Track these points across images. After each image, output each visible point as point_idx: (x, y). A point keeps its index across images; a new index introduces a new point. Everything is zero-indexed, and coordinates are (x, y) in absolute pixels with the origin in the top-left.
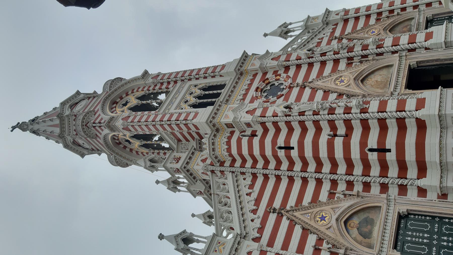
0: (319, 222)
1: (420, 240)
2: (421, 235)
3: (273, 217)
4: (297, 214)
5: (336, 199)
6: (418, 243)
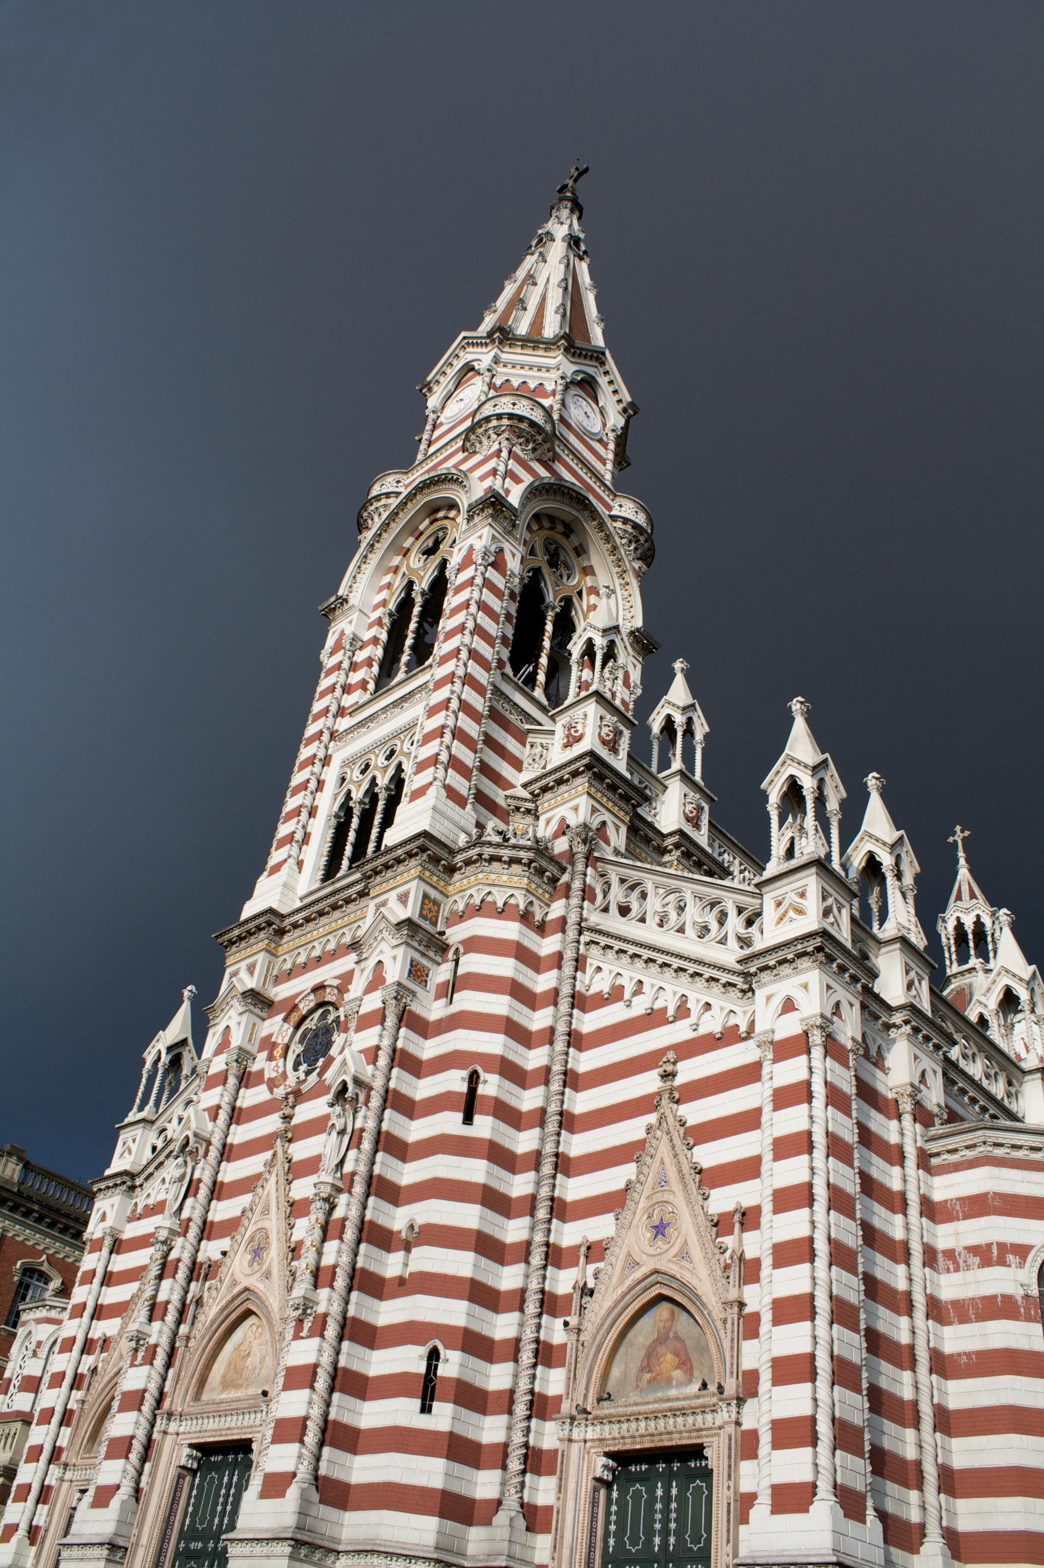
1: (658, 1526)
2: (673, 1525)
3: (648, 1082)
4: (663, 1150)
5: (719, 1240)
6: (650, 1521)
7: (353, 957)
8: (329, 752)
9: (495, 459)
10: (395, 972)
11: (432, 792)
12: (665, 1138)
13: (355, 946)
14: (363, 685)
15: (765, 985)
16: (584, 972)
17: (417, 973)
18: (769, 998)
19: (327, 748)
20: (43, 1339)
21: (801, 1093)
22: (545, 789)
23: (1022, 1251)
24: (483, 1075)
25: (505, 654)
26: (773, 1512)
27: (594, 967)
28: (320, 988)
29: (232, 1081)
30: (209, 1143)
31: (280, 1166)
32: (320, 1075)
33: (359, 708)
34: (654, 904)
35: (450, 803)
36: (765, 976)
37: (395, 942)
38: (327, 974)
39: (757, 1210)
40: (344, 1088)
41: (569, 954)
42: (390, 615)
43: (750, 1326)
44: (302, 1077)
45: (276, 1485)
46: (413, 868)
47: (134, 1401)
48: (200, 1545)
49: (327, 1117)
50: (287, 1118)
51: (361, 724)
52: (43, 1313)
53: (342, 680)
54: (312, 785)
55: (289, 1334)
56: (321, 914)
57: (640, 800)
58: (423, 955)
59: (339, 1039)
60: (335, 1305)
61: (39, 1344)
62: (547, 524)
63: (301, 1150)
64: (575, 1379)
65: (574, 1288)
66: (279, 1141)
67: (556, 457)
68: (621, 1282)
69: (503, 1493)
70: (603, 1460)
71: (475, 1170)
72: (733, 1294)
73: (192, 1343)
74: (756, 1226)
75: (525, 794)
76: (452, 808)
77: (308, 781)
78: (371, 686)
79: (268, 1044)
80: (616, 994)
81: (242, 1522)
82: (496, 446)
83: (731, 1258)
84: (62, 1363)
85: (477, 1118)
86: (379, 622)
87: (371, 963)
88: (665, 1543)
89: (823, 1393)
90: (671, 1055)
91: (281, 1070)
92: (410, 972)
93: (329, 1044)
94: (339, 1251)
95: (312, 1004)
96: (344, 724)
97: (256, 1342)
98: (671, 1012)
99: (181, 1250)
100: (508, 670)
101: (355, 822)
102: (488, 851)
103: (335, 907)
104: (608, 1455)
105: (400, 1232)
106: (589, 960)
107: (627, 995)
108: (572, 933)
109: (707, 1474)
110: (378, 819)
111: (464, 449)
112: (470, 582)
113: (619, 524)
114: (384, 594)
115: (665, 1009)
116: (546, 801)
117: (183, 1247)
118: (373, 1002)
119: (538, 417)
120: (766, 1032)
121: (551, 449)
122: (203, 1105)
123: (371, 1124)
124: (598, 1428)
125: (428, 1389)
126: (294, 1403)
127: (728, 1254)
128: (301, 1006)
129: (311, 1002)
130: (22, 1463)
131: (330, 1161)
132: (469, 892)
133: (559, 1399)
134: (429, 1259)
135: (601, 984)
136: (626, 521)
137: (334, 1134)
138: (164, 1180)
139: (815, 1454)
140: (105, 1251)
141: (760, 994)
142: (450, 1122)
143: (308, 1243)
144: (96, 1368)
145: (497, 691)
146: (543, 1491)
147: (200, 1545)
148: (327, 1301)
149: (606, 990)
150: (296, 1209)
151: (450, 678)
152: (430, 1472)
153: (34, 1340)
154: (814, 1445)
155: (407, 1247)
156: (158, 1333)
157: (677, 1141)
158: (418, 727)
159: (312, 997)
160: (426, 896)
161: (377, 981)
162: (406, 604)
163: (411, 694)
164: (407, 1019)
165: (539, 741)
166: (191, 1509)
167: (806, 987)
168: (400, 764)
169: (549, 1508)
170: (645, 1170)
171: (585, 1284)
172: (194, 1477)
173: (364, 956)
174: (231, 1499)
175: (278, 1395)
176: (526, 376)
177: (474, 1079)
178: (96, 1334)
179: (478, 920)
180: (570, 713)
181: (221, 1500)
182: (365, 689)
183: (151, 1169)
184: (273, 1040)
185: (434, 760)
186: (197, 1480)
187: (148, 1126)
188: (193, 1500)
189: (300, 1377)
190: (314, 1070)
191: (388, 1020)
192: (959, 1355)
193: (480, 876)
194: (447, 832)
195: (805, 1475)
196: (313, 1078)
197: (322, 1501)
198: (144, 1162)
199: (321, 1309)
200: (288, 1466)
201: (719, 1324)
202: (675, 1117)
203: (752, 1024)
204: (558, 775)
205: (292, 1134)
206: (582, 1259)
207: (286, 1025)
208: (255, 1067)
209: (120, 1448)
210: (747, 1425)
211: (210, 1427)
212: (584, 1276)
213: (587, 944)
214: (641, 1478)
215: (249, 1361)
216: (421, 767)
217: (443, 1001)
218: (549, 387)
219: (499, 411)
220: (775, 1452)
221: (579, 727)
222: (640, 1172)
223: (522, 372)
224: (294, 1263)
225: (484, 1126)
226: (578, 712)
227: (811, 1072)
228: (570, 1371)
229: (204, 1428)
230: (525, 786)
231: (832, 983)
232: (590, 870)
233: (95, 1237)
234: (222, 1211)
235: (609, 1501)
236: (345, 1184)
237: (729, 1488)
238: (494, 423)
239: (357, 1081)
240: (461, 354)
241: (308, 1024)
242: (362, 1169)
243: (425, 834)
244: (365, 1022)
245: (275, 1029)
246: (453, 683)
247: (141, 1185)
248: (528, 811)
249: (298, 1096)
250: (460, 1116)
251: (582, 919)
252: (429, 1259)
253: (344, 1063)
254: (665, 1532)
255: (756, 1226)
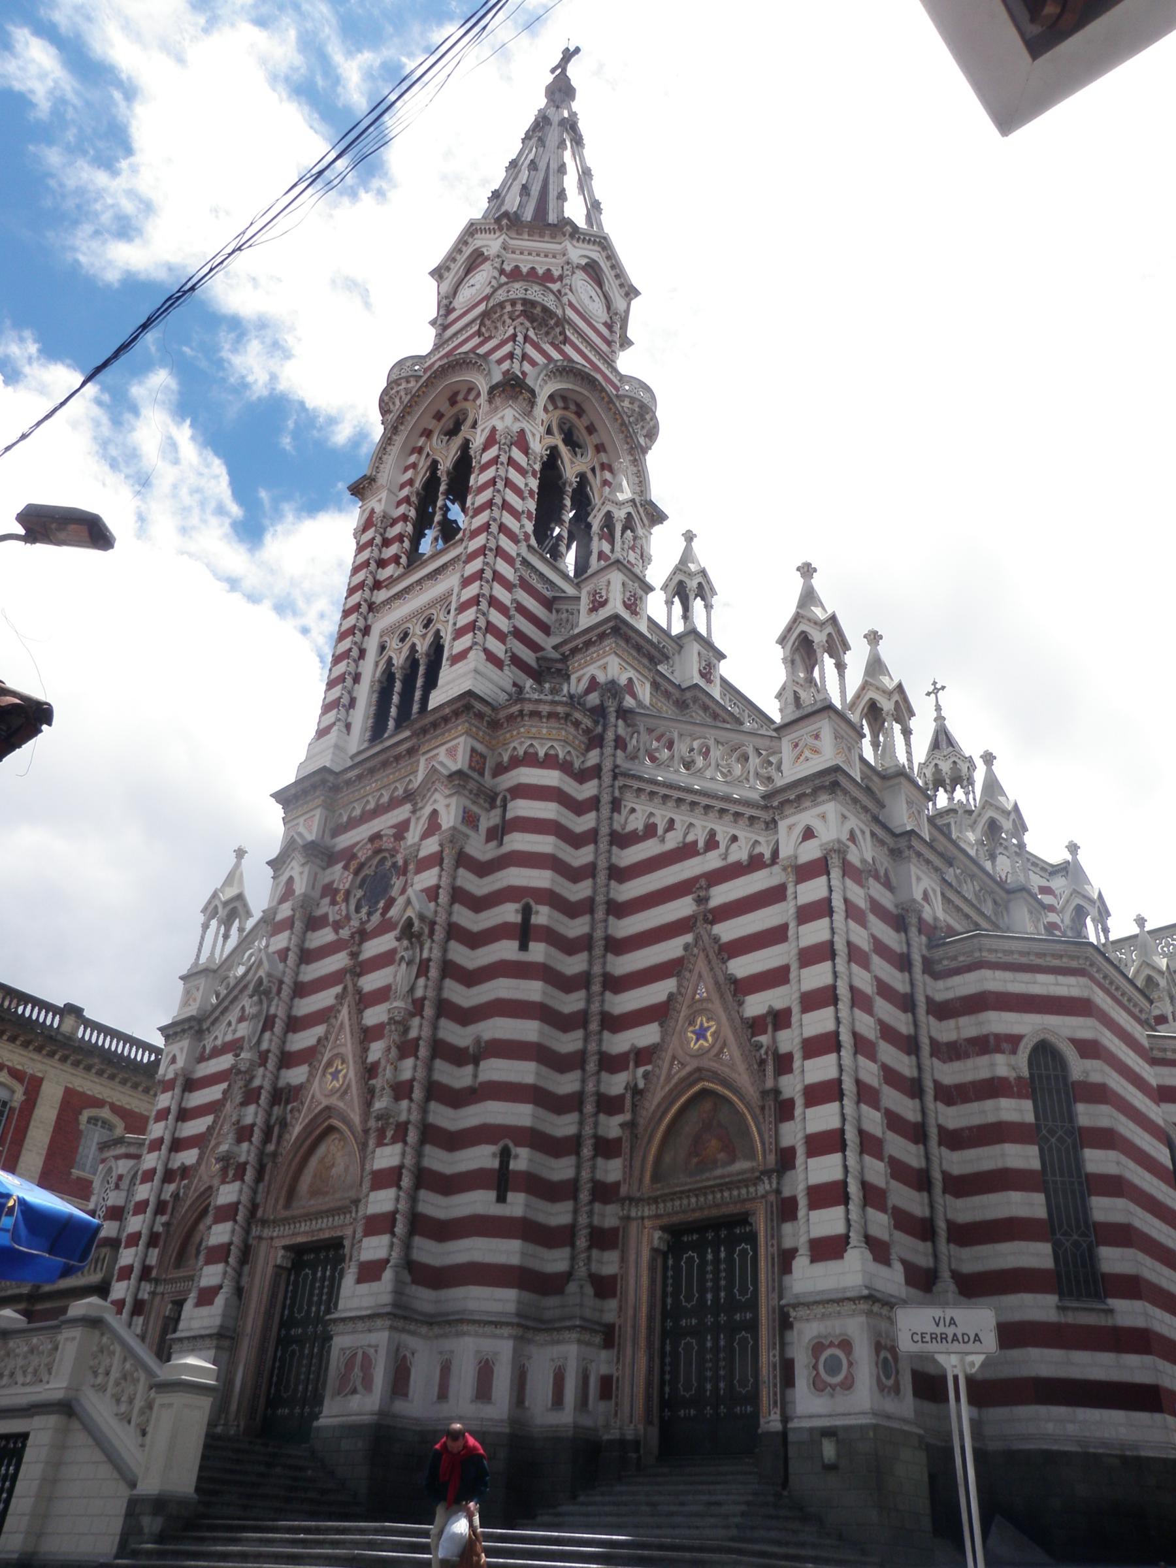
0: (691, 1029)
1: (709, 1284)
3: (683, 907)
4: (701, 965)
6: (702, 1280)
7: (408, 807)
8: (369, 622)
9: (511, 343)
10: (448, 820)
11: (472, 655)
12: (702, 955)
13: (409, 796)
14: (396, 559)
15: (787, 817)
16: (619, 813)
17: (470, 819)
18: (790, 828)
19: (366, 619)
20: (125, 1172)
21: (823, 909)
22: (575, 651)
23: (1014, 1041)
24: (535, 907)
25: (529, 527)
26: (812, 1261)
27: (628, 808)
28: (376, 837)
29: (298, 925)
30: (281, 982)
31: (349, 999)
32: (383, 914)
33: (392, 581)
34: (681, 748)
35: (490, 665)
36: (788, 810)
37: (447, 792)
38: (384, 823)
39: (788, 1012)
40: (409, 923)
41: (606, 798)
42: (418, 494)
43: (785, 1110)
44: (365, 918)
45: (370, 1272)
46: (461, 725)
47: (228, 1213)
48: (300, 1331)
49: (393, 952)
50: (354, 955)
51: (398, 596)
52: (121, 1150)
53: (376, 554)
54: (355, 653)
55: (372, 1143)
56: (372, 771)
57: (661, 658)
58: (474, 802)
59: (397, 883)
60: (415, 1113)
61: (120, 1177)
62: (560, 404)
63: (371, 982)
64: (631, 1166)
65: (626, 1088)
66: (348, 976)
67: (566, 340)
68: (669, 1077)
69: (572, 1267)
70: (657, 1234)
71: (533, 990)
72: (769, 1084)
73: (280, 1159)
74: (788, 1025)
75: (556, 655)
76: (490, 669)
77: (350, 650)
78: (404, 560)
79: (329, 891)
80: (650, 831)
81: (341, 1306)
82: (511, 331)
83: (766, 1053)
84: (143, 1192)
85: (532, 945)
86: (407, 500)
87: (427, 811)
88: (716, 1298)
89: (852, 1161)
90: (703, 882)
91: (344, 913)
92: (464, 818)
93: (388, 887)
94: (415, 1068)
95: (370, 852)
96: (381, 596)
97: (339, 1154)
98: (701, 844)
99: (261, 1078)
100: (533, 542)
101: (398, 686)
102: (528, 707)
103: (385, 764)
104: (663, 1229)
105: (467, 1048)
106: (623, 803)
107: (660, 831)
108: (607, 779)
109: (752, 1238)
110: (420, 682)
111: (479, 333)
112: (495, 461)
113: (626, 404)
114: (409, 474)
115: (695, 843)
116: (574, 663)
117: (264, 1076)
118: (431, 846)
119: (550, 302)
120: (789, 857)
121: (563, 333)
122: (272, 949)
123: (436, 954)
124: (654, 1207)
125: (502, 1181)
126: (382, 1201)
127: (763, 1051)
128: (360, 854)
129: (368, 850)
130: (113, 1283)
131: (402, 986)
132: (512, 745)
133: (617, 1185)
134: (496, 1070)
135: (636, 823)
136: (633, 400)
137: (404, 966)
138: (229, 1024)
139: (847, 1212)
140: (178, 1090)
141: (783, 825)
142: (507, 950)
143: (383, 1062)
144: (178, 1194)
145: (525, 562)
146: (608, 1263)
147: (300, 1331)
148: (405, 1110)
149: (641, 827)
150: (367, 1035)
151: (482, 551)
152: (506, 1251)
153: (114, 1174)
154: (846, 1204)
155: (476, 1060)
156: (246, 1152)
157: (712, 955)
158: (454, 598)
159: (369, 846)
160: (473, 750)
161: (433, 826)
162: (432, 483)
163: (444, 567)
164: (463, 860)
165: (565, 607)
166: (288, 1302)
167: (823, 817)
168: (438, 631)
169: (613, 1278)
170: (685, 983)
171: (636, 1085)
172: (289, 1275)
173: (420, 805)
174: (326, 1290)
175: (367, 1195)
176: (533, 262)
177: (527, 912)
178: (175, 1164)
179: (523, 770)
180: (594, 580)
181: (317, 1291)
182: (398, 563)
183: (217, 1013)
184: (335, 886)
185: (472, 627)
186: (292, 1278)
187: (211, 975)
188: (289, 1294)
189: (386, 1178)
190: (376, 910)
191: (446, 861)
192: (962, 1129)
193: (522, 730)
194: (489, 692)
195: (839, 1229)
196: (376, 918)
197: (414, 1282)
198: (209, 1008)
199: (403, 1117)
200: (381, 1254)
201: (758, 1111)
202: (709, 935)
203: (775, 854)
204: (587, 637)
205: (361, 968)
206: (631, 1065)
207: (347, 873)
208: (319, 912)
209: (219, 1254)
210: (787, 1193)
211: (302, 1229)
212: (635, 1078)
213: (620, 788)
214: (692, 1246)
215: (334, 1171)
216: (459, 633)
217: (494, 844)
218: (556, 273)
219: (512, 296)
220: (811, 1213)
221: (604, 593)
222: (680, 986)
223: (530, 258)
224: (371, 1082)
225: (538, 952)
226: (601, 581)
227: (831, 891)
228: (625, 1160)
229: (297, 1230)
230: (555, 648)
231: (847, 814)
232: (620, 722)
233: (167, 1078)
234: (302, 1040)
235: (665, 1268)
236: (418, 1006)
237: (772, 1246)
238: (509, 308)
239: (422, 918)
240: (470, 240)
241: (366, 871)
242: (431, 994)
243: (470, 693)
244: (424, 865)
245: (337, 876)
246: (485, 555)
247: (208, 1029)
248: (559, 671)
249: (363, 935)
250: (515, 944)
251: (616, 766)
252: (496, 1070)
253: (408, 902)
254: (716, 1289)
255: (788, 1025)
